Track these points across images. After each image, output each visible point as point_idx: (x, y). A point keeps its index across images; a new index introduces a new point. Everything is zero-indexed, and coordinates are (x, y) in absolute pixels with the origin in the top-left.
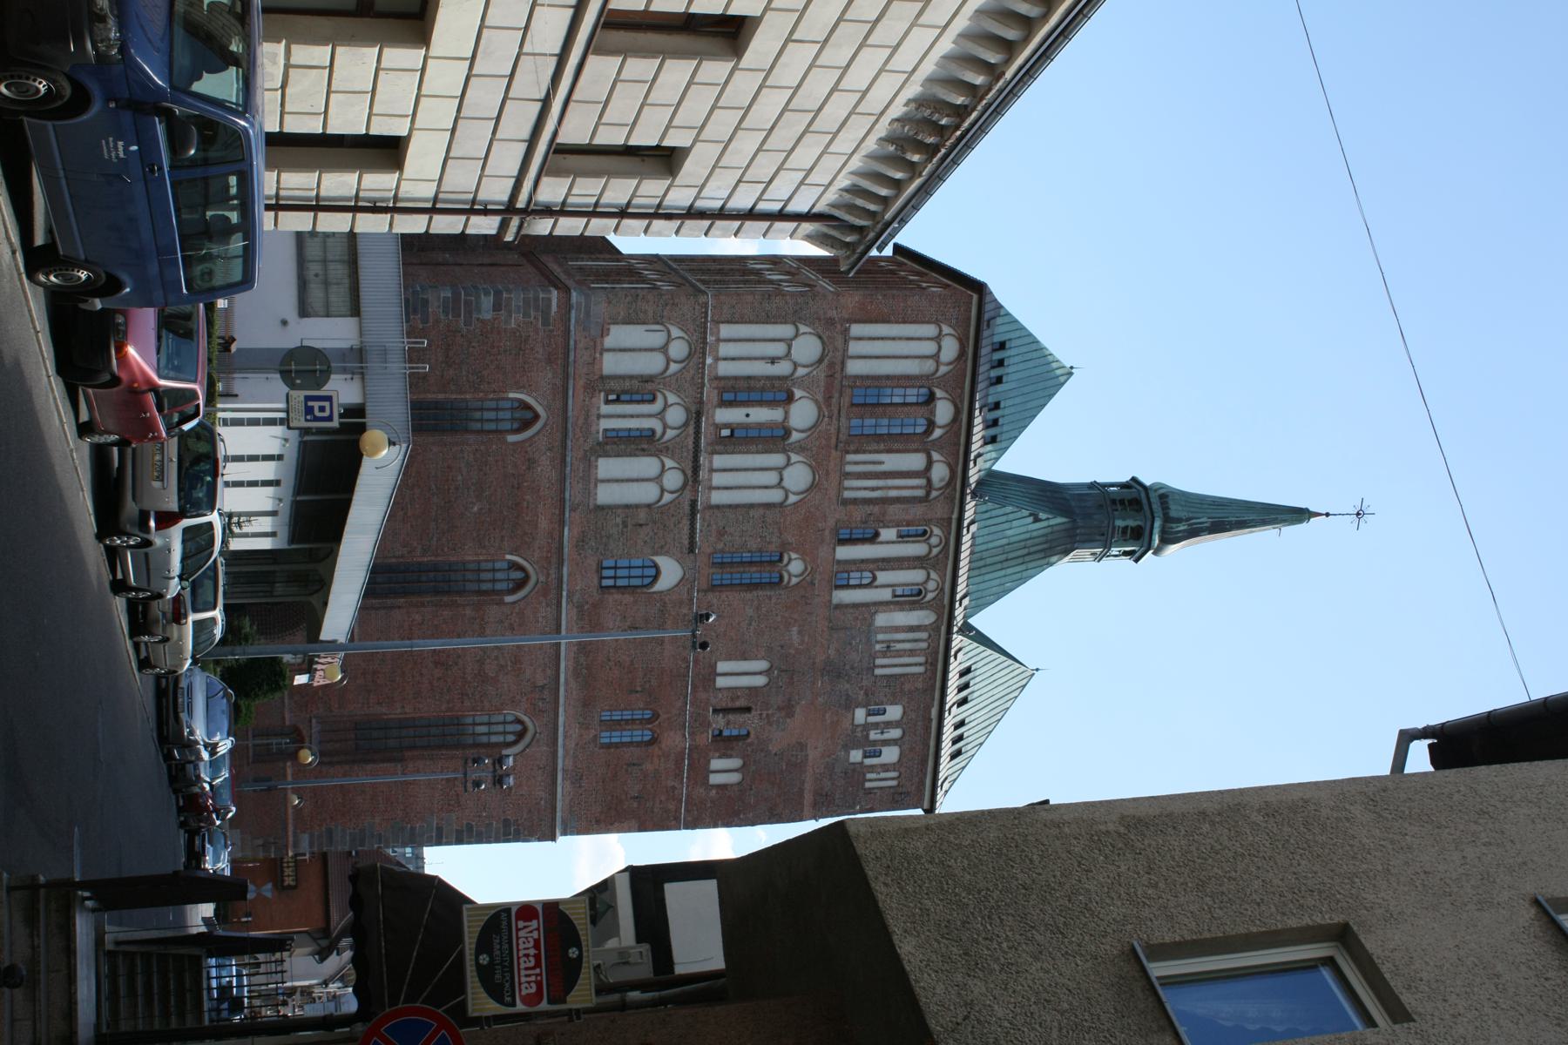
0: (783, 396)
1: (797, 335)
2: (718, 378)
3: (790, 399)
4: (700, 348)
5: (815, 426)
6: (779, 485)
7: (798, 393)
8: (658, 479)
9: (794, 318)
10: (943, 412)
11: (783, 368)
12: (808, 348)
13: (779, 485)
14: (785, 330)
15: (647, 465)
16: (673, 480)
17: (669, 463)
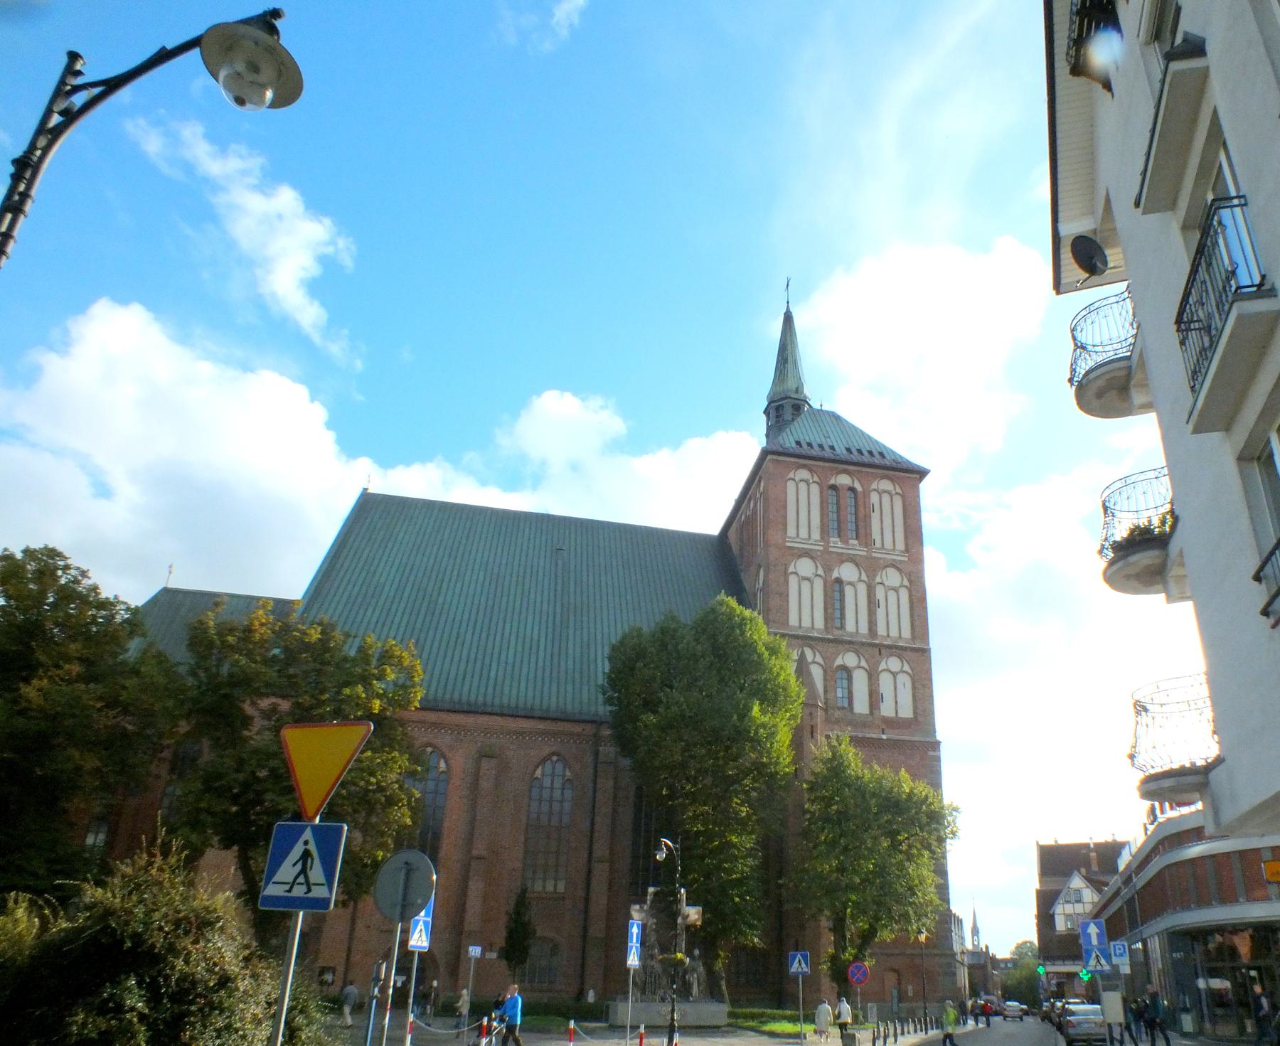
0: (837, 587)
1: (796, 573)
2: (826, 628)
3: (839, 581)
4: (806, 640)
5: (857, 565)
6: (895, 590)
7: (835, 575)
8: (894, 675)
9: (786, 574)
10: (843, 480)
11: (819, 584)
12: (805, 567)
13: (895, 590)
14: (793, 581)
15: (885, 683)
16: (894, 663)
17: (883, 666)
